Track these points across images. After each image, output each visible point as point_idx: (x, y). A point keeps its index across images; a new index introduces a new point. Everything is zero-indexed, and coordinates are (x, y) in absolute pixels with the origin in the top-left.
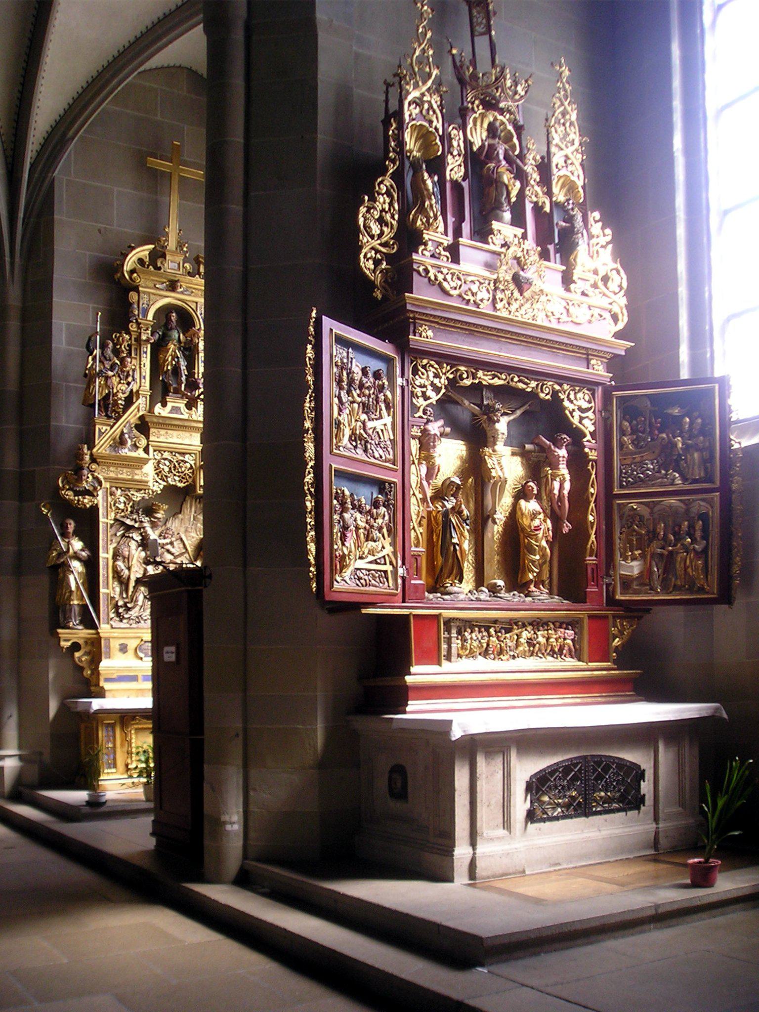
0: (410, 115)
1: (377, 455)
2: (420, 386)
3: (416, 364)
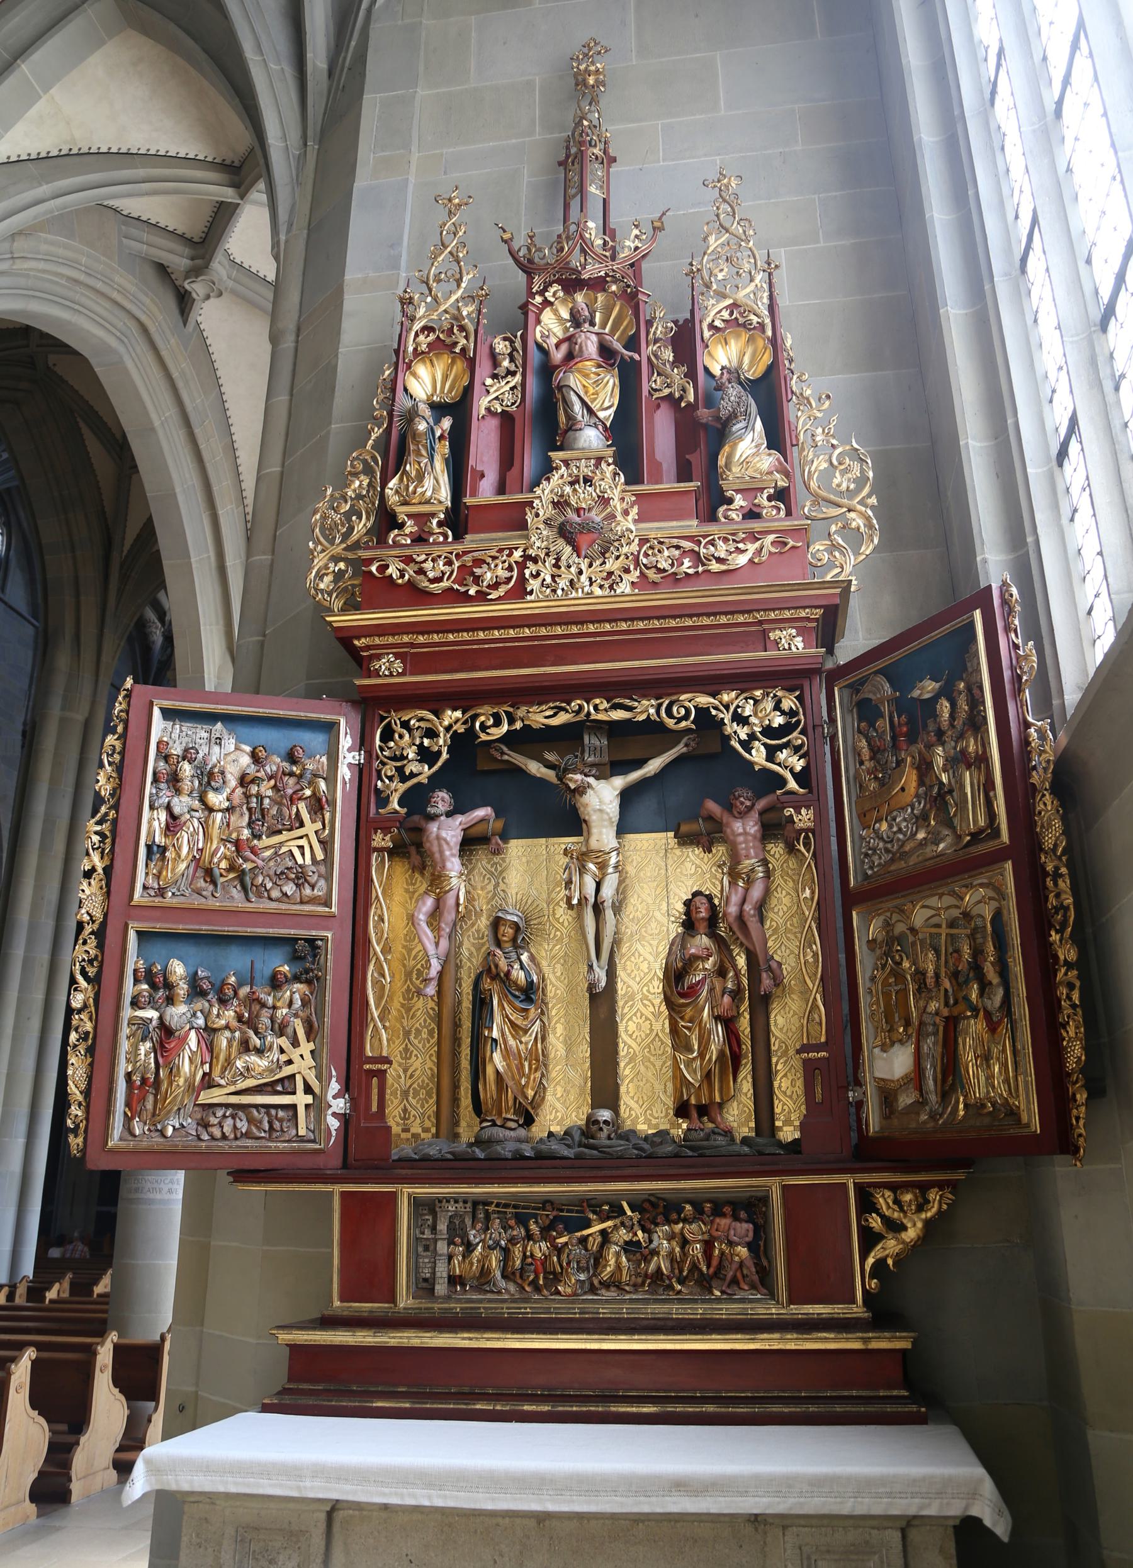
0: (415, 350)
1: (275, 894)
2: (394, 758)
3: (390, 722)
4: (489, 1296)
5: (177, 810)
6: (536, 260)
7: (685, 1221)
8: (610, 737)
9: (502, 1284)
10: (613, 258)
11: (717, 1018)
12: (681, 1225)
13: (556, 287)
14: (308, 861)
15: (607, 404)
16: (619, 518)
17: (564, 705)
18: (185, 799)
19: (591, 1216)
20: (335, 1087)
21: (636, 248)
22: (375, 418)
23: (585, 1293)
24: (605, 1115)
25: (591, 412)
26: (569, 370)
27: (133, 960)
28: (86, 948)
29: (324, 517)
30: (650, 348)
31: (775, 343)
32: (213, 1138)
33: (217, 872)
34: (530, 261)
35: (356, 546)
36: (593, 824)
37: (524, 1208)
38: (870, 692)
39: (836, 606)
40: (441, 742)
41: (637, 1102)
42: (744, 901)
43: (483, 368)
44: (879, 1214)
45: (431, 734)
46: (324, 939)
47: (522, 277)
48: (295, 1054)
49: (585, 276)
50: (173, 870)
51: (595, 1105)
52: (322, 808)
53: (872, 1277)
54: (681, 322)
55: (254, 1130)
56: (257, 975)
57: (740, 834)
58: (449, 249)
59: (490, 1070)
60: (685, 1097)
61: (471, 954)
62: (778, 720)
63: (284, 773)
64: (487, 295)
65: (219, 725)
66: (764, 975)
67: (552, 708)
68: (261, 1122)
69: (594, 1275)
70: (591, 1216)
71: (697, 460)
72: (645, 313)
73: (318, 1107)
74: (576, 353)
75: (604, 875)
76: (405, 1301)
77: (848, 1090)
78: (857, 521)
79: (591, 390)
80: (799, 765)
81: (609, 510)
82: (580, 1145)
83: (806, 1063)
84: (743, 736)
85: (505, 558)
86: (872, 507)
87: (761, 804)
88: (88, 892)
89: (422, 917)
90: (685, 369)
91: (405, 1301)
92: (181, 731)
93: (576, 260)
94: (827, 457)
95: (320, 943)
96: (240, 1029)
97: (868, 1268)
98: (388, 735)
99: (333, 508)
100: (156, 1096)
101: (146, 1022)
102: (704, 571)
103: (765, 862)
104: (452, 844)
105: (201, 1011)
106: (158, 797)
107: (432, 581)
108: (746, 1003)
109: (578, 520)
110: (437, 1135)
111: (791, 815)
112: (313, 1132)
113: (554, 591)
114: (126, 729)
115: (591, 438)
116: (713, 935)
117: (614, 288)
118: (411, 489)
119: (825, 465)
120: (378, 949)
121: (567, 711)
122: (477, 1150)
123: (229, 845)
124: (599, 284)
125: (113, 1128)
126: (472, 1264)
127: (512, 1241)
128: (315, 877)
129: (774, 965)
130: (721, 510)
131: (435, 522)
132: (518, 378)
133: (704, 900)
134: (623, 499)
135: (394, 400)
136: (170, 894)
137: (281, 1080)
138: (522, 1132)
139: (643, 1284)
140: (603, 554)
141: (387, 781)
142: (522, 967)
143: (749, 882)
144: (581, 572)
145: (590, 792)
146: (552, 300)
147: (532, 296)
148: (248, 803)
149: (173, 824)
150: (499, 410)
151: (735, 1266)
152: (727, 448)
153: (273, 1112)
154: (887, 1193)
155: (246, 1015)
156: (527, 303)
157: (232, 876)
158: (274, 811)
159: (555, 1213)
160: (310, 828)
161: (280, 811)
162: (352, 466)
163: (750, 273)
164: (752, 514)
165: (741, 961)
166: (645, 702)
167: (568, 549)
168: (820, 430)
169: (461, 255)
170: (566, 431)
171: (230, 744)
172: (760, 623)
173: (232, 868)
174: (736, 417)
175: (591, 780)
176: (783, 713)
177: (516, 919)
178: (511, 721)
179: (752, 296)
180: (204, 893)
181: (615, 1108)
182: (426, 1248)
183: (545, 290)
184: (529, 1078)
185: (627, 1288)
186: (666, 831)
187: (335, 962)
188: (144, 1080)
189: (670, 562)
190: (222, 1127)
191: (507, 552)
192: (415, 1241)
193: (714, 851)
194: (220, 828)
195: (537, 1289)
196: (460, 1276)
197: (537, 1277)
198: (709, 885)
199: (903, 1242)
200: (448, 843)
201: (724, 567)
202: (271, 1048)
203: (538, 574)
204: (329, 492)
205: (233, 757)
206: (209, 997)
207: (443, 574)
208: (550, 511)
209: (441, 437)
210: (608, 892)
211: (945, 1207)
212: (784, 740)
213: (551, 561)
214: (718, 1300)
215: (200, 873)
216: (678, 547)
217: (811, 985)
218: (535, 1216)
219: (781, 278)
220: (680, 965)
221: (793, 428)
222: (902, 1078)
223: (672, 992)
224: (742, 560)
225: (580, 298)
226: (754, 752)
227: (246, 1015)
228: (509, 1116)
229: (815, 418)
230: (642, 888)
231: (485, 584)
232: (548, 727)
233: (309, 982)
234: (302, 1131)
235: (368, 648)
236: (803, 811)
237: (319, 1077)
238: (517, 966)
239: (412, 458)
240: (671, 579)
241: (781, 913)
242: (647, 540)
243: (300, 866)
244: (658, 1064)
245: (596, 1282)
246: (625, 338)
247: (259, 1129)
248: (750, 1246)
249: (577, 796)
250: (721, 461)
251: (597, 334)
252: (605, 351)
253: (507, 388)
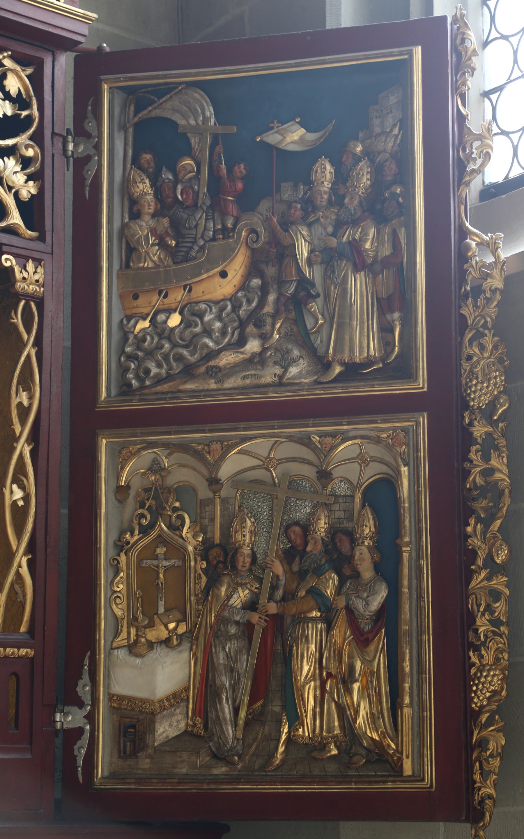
38: (175, 110)
212: (10, 142)
222: (168, 699)
236: (30, 266)
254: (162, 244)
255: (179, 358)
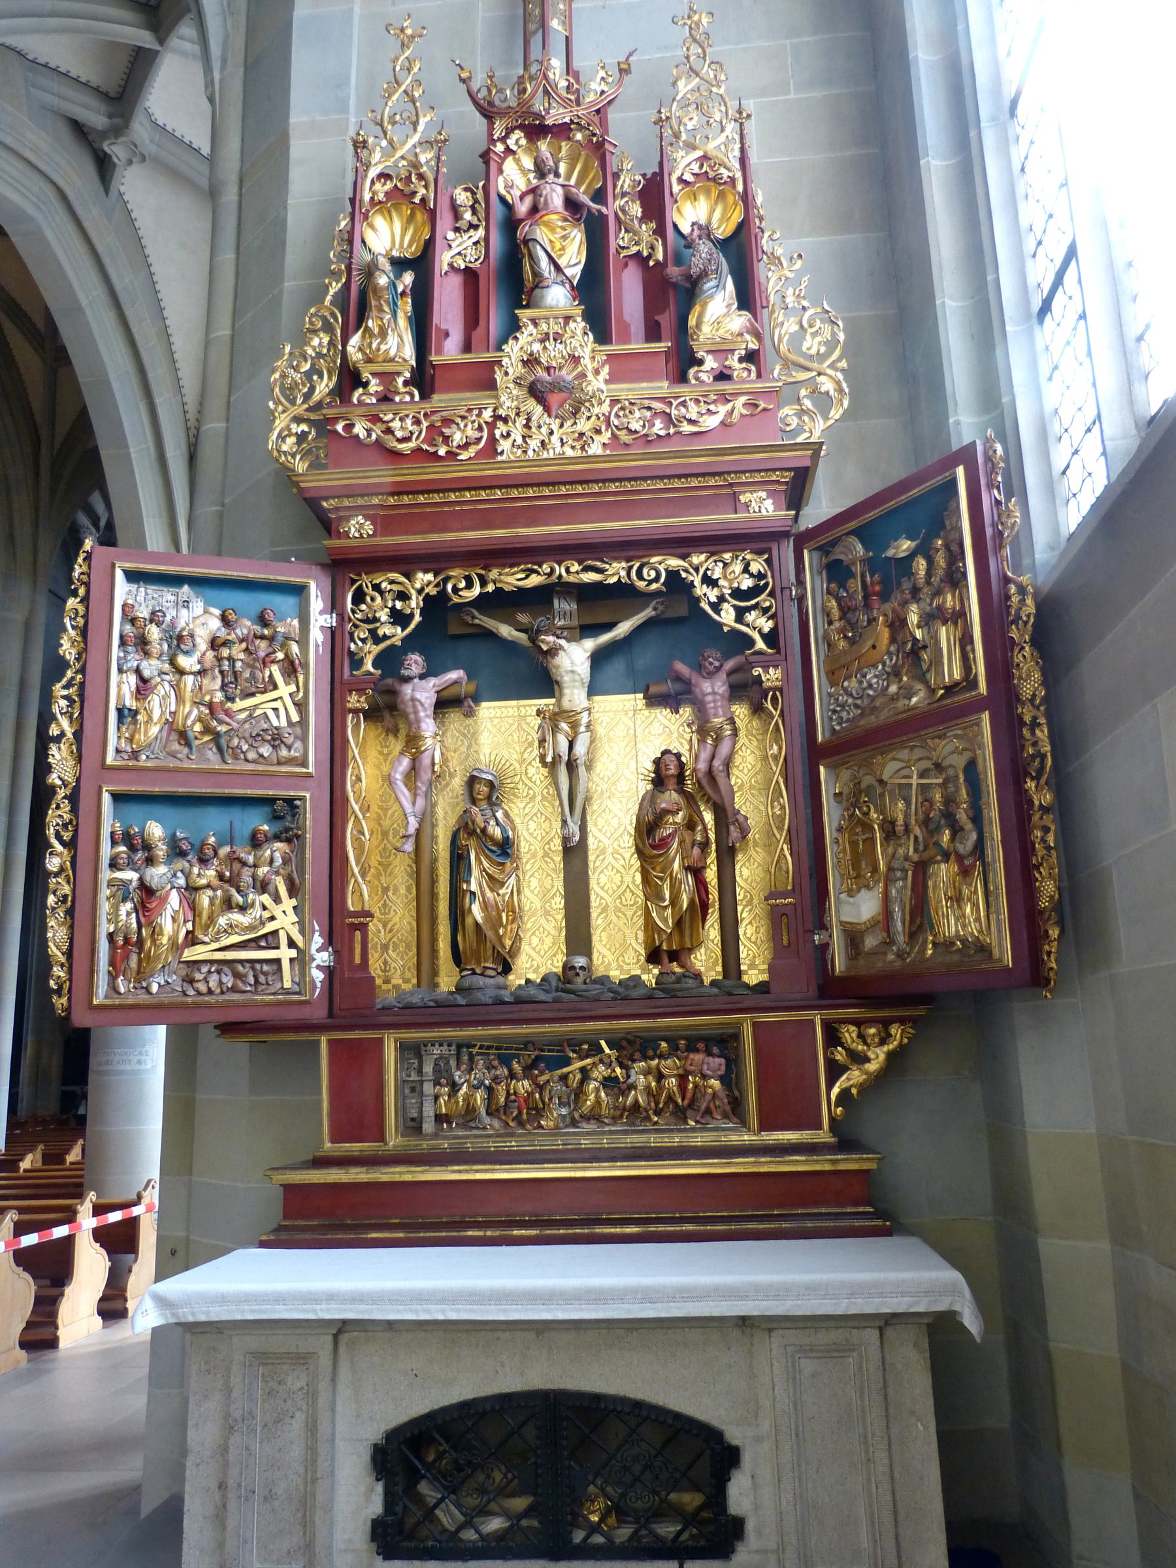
0: (372, 199)
1: (252, 755)
2: (367, 621)
3: (361, 585)
4: (475, 1132)
5: (146, 673)
6: (497, 103)
7: (661, 1057)
8: (579, 601)
9: (487, 1120)
10: (578, 103)
11: (688, 869)
12: (656, 1061)
13: (518, 134)
14: (284, 723)
15: (573, 261)
16: (590, 377)
17: (536, 567)
18: (154, 662)
19: (572, 1055)
20: (318, 940)
21: (603, 92)
22: (333, 273)
23: (567, 1126)
24: (580, 961)
25: (558, 268)
26: (536, 223)
27: (109, 822)
28: (59, 812)
29: (284, 376)
30: (617, 203)
31: (746, 198)
32: (199, 993)
33: (191, 735)
34: (491, 104)
35: (319, 406)
36: (565, 685)
37: (506, 1049)
39: (807, 469)
40: (413, 604)
41: (609, 950)
42: (713, 757)
43: (444, 220)
44: (843, 1048)
45: (403, 596)
46: (303, 799)
47: (480, 122)
48: (277, 911)
49: (549, 122)
50: (146, 733)
51: (571, 951)
52: (295, 671)
53: (837, 1106)
54: (649, 176)
55: (240, 984)
56: (237, 836)
57: (709, 694)
58: (403, 87)
59: (469, 921)
60: (657, 943)
61: (446, 813)
62: (747, 583)
63: (256, 637)
64: (446, 140)
65: (186, 588)
66: (732, 828)
67: (523, 571)
68: (246, 976)
69: (575, 1109)
70: (572, 1055)
71: (666, 320)
72: (613, 164)
73: (302, 960)
74: (541, 206)
75: (576, 734)
76: (394, 1140)
77: (814, 933)
78: (827, 385)
79: (558, 246)
80: (767, 626)
81: (580, 369)
82: (557, 990)
83: (774, 907)
84: (713, 599)
85: (474, 418)
86: (843, 371)
87: (730, 665)
88: (58, 757)
89: (398, 776)
90: (653, 225)
91: (394, 1140)
92: (147, 594)
93: (539, 106)
94: (797, 319)
95: (298, 803)
96: (222, 888)
97: (833, 1097)
98: (359, 598)
99: (293, 367)
100: (139, 954)
101: (125, 884)
102: (676, 433)
103: (732, 721)
104: (426, 705)
105: (182, 871)
106: (127, 661)
107: (400, 441)
108: (713, 855)
109: (548, 378)
110: (419, 984)
111: (760, 675)
112: (298, 984)
113: (525, 452)
114: (88, 592)
115: (557, 296)
116: (681, 791)
117: (579, 136)
118: (374, 346)
119: (796, 328)
120: (356, 808)
121: (539, 574)
122: (458, 997)
123: (202, 708)
124: (562, 131)
125: (98, 987)
126: (457, 1103)
127: (496, 1080)
128: (291, 739)
129: (741, 819)
130: (692, 372)
131: (400, 380)
132: (481, 232)
133: (673, 758)
134: (593, 358)
135: (351, 252)
136: (144, 757)
137: (265, 936)
138: (500, 979)
139: (621, 1116)
140: (574, 415)
141: (360, 644)
142: (498, 823)
143: (718, 740)
144: (551, 433)
145: (561, 653)
146: (514, 148)
147: (493, 142)
148: (220, 666)
149: (144, 686)
150: (463, 267)
151: (708, 1098)
152: (697, 309)
153: (258, 966)
154: (852, 1028)
155: (228, 874)
156: (488, 151)
157: (206, 738)
158: (247, 674)
159: (536, 1053)
160: (285, 690)
161: (253, 675)
162: (311, 323)
163: (721, 122)
164: (722, 376)
165: (708, 817)
166: (615, 565)
167: (539, 409)
168: (790, 291)
169: (416, 94)
170: (532, 289)
171: (198, 606)
172: (731, 485)
173: (207, 730)
174: (707, 275)
175: (562, 642)
176: (752, 575)
177: (490, 778)
178: (484, 583)
179: (723, 148)
180: (179, 756)
181: (588, 954)
182: (413, 1090)
183: (507, 136)
184: (505, 927)
185: (606, 1121)
186: (635, 692)
187: (314, 819)
188: (127, 940)
189: (641, 423)
190: (208, 982)
191: (476, 412)
192: (401, 1084)
193: (681, 711)
194: (192, 691)
195: (521, 1124)
196: (446, 1115)
197: (520, 1113)
198: (676, 744)
199: (867, 1073)
200: (422, 704)
201: (694, 429)
202: (253, 905)
203: (508, 435)
204: (288, 349)
205: (202, 620)
206: (189, 857)
207: (412, 433)
208: (521, 370)
209: (403, 294)
210: (580, 749)
211: (906, 1041)
212: (753, 602)
213: (522, 421)
214: (693, 1130)
215: (174, 736)
216: (649, 408)
217: (778, 837)
218: (517, 1056)
219: (751, 127)
220: (651, 818)
221: (763, 288)
223: (644, 844)
224: (712, 422)
225: (543, 146)
226: (723, 613)
227: (228, 874)
228: (487, 965)
229: (787, 279)
230: (612, 748)
231: (455, 444)
232: (521, 590)
233: (288, 841)
234: (287, 984)
235: (337, 509)
236: (771, 670)
237: (302, 932)
238: (492, 822)
239: (374, 313)
240: (643, 440)
241: (746, 771)
242: (618, 401)
243: (276, 728)
244: (630, 914)
245: (577, 1116)
246: (591, 191)
247: (244, 982)
248: (722, 1079)
249: (549, 658)
250: (692, 322)
251: (563, 186)
252: (571, 204)
253: (470, 242)
254: (846, 637)
255: (857, 706)
